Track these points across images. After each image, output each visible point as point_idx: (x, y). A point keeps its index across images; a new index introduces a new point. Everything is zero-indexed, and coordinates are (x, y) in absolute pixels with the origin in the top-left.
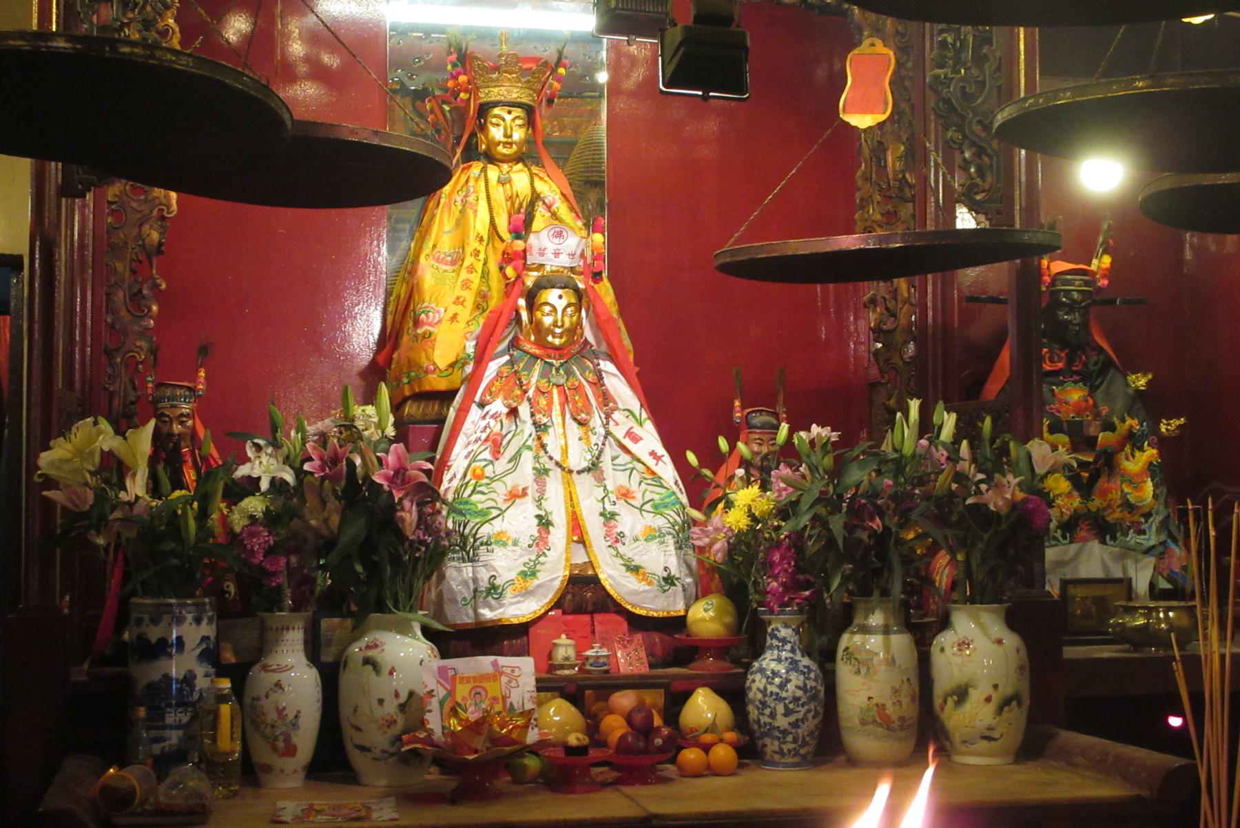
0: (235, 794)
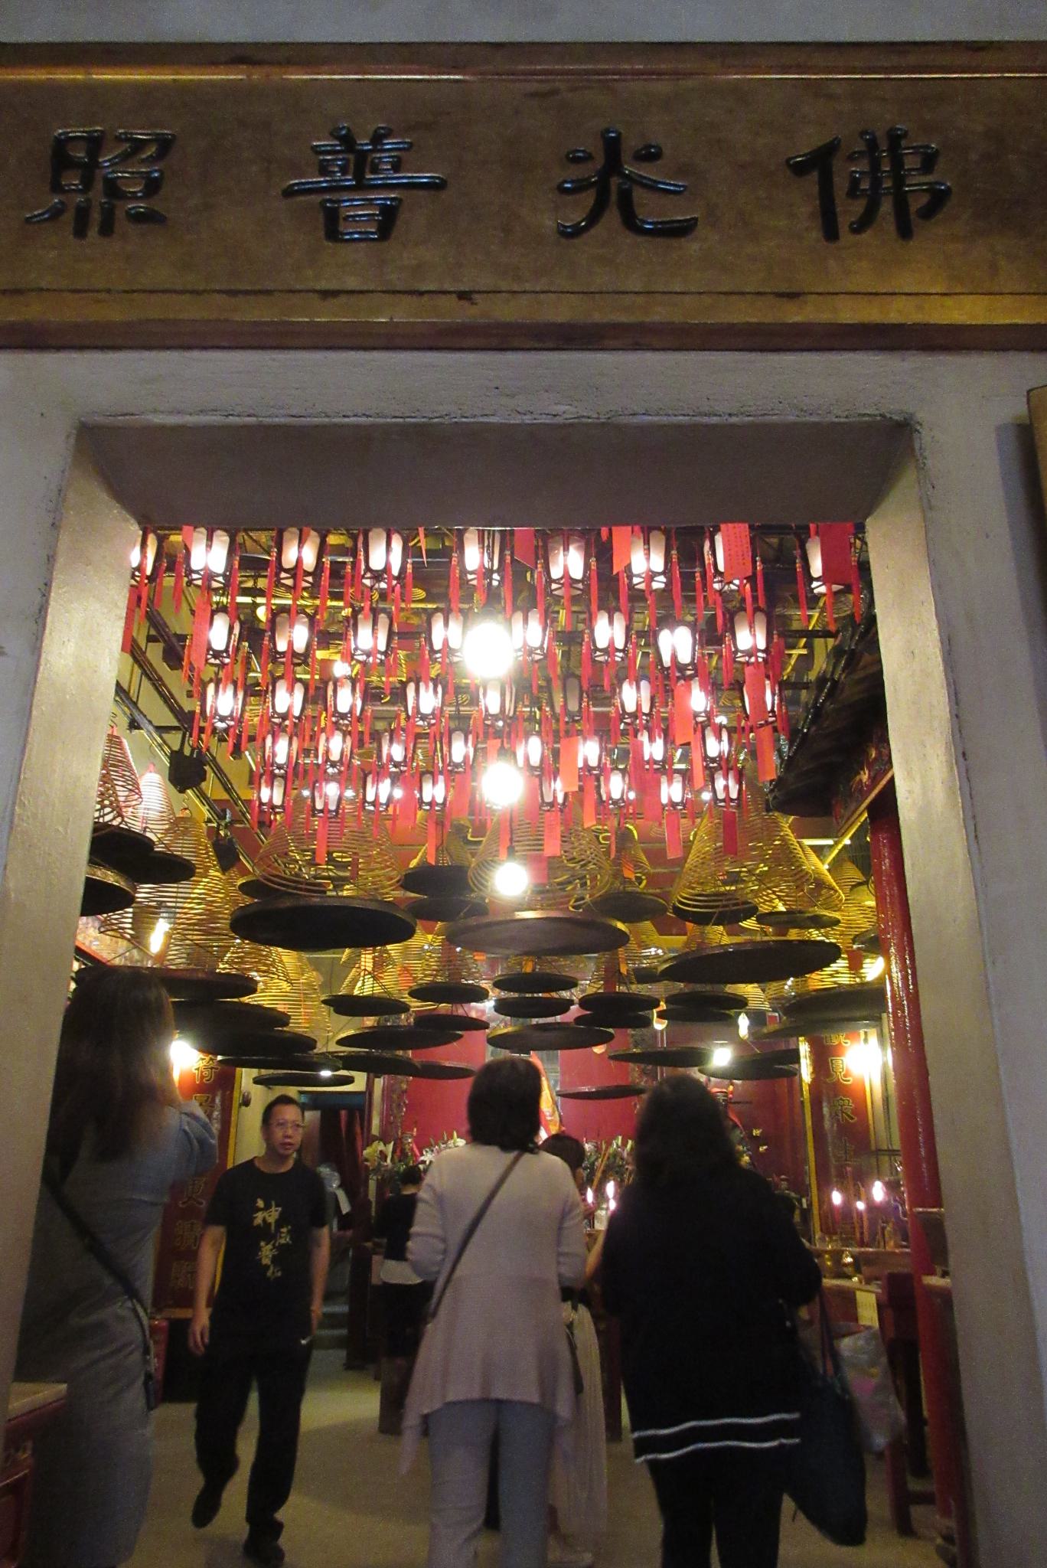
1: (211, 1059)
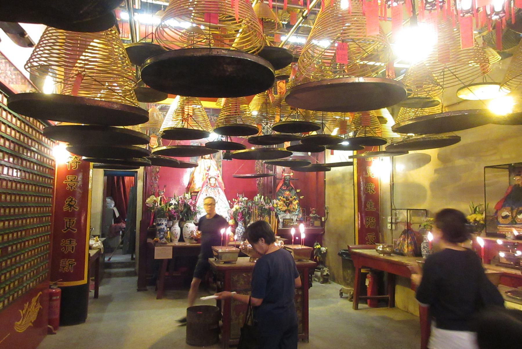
1: (76, 157)
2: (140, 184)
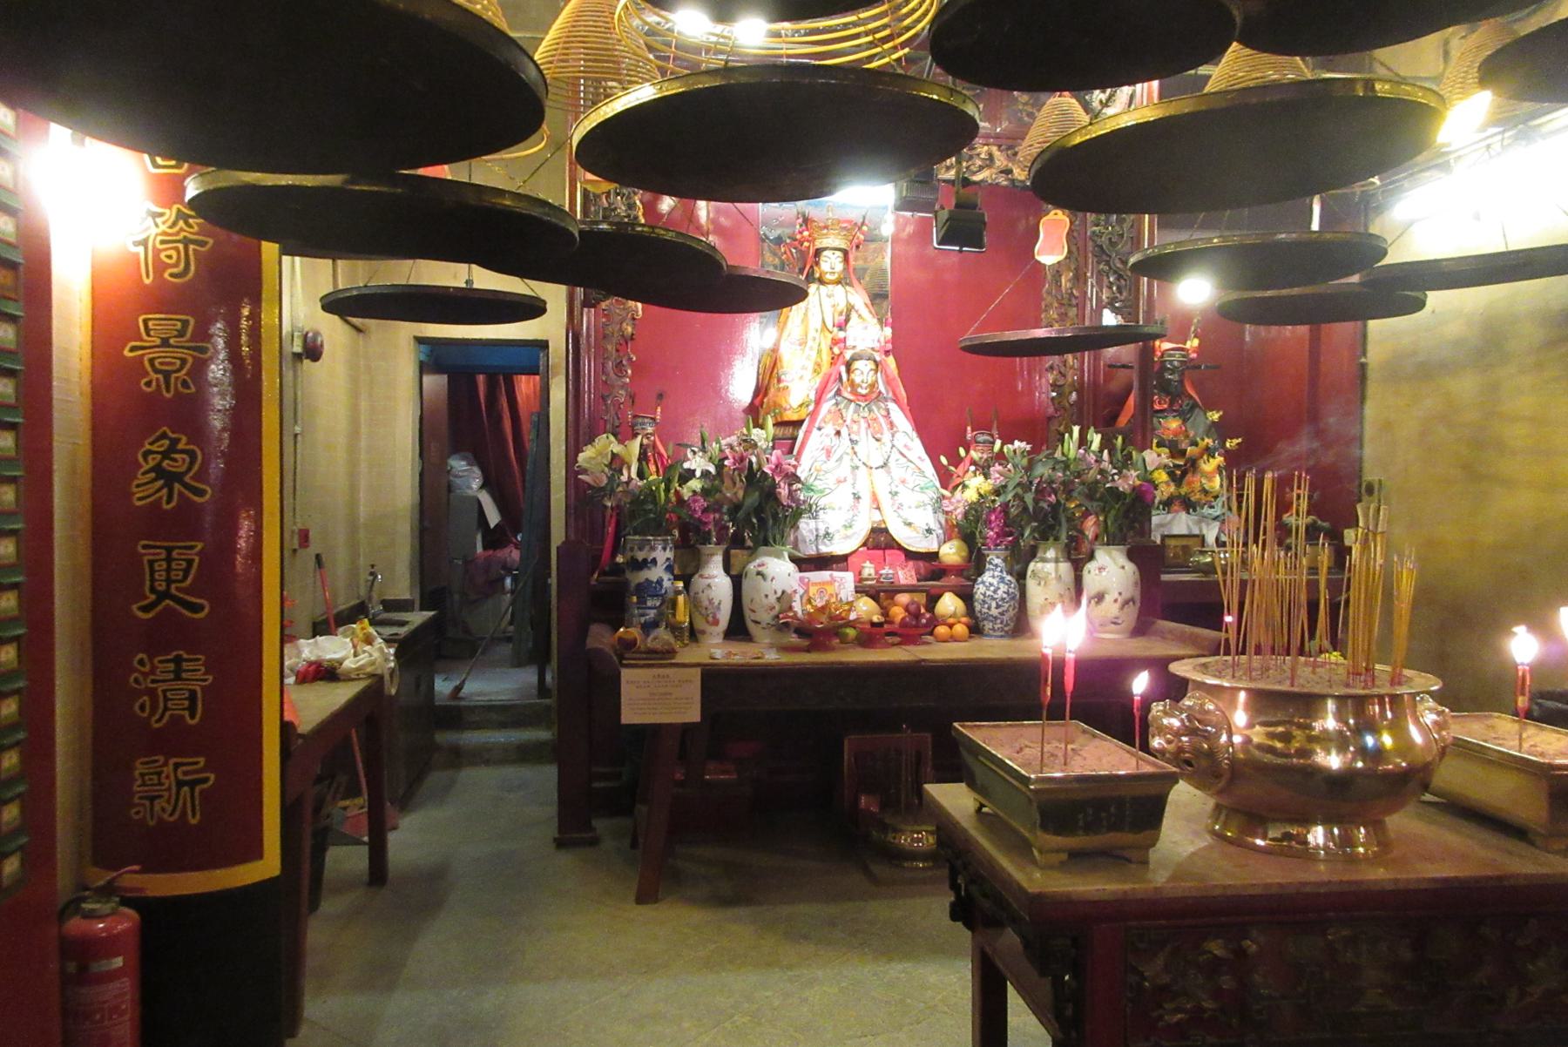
0: (686, 645)
2: (558, 395)
